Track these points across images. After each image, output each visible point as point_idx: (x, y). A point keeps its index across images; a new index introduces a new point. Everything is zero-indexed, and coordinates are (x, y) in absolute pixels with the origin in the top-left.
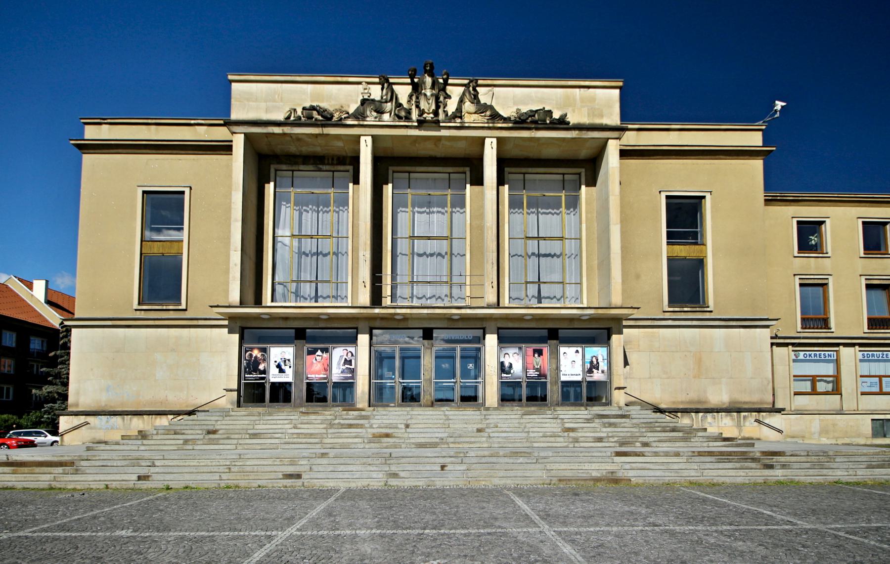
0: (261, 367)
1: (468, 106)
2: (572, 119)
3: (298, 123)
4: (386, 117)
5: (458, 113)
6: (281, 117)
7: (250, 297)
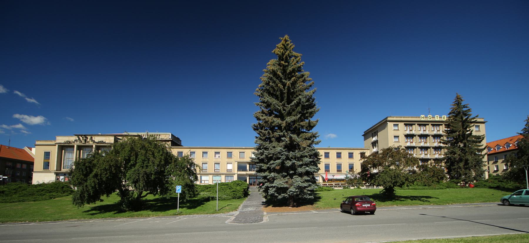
0: (59, 179)
1: (90, 141)
2: (106, 142)
3: (65, 143)
4: (78, 142)
5: (89, 142)
6: (63, 142)
7: (59, 169)
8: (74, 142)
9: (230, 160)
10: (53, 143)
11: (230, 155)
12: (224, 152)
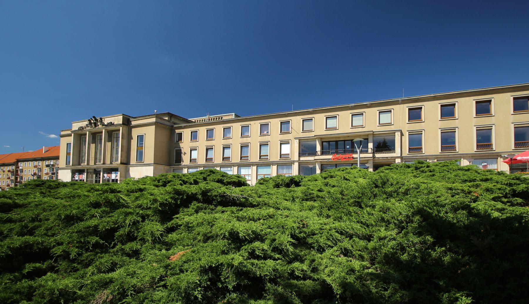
4: (89, 127)
8: (85, 128)
9: (285, 137)
10: (69, 132)
11: (285, 127)
12: (275, 124)
